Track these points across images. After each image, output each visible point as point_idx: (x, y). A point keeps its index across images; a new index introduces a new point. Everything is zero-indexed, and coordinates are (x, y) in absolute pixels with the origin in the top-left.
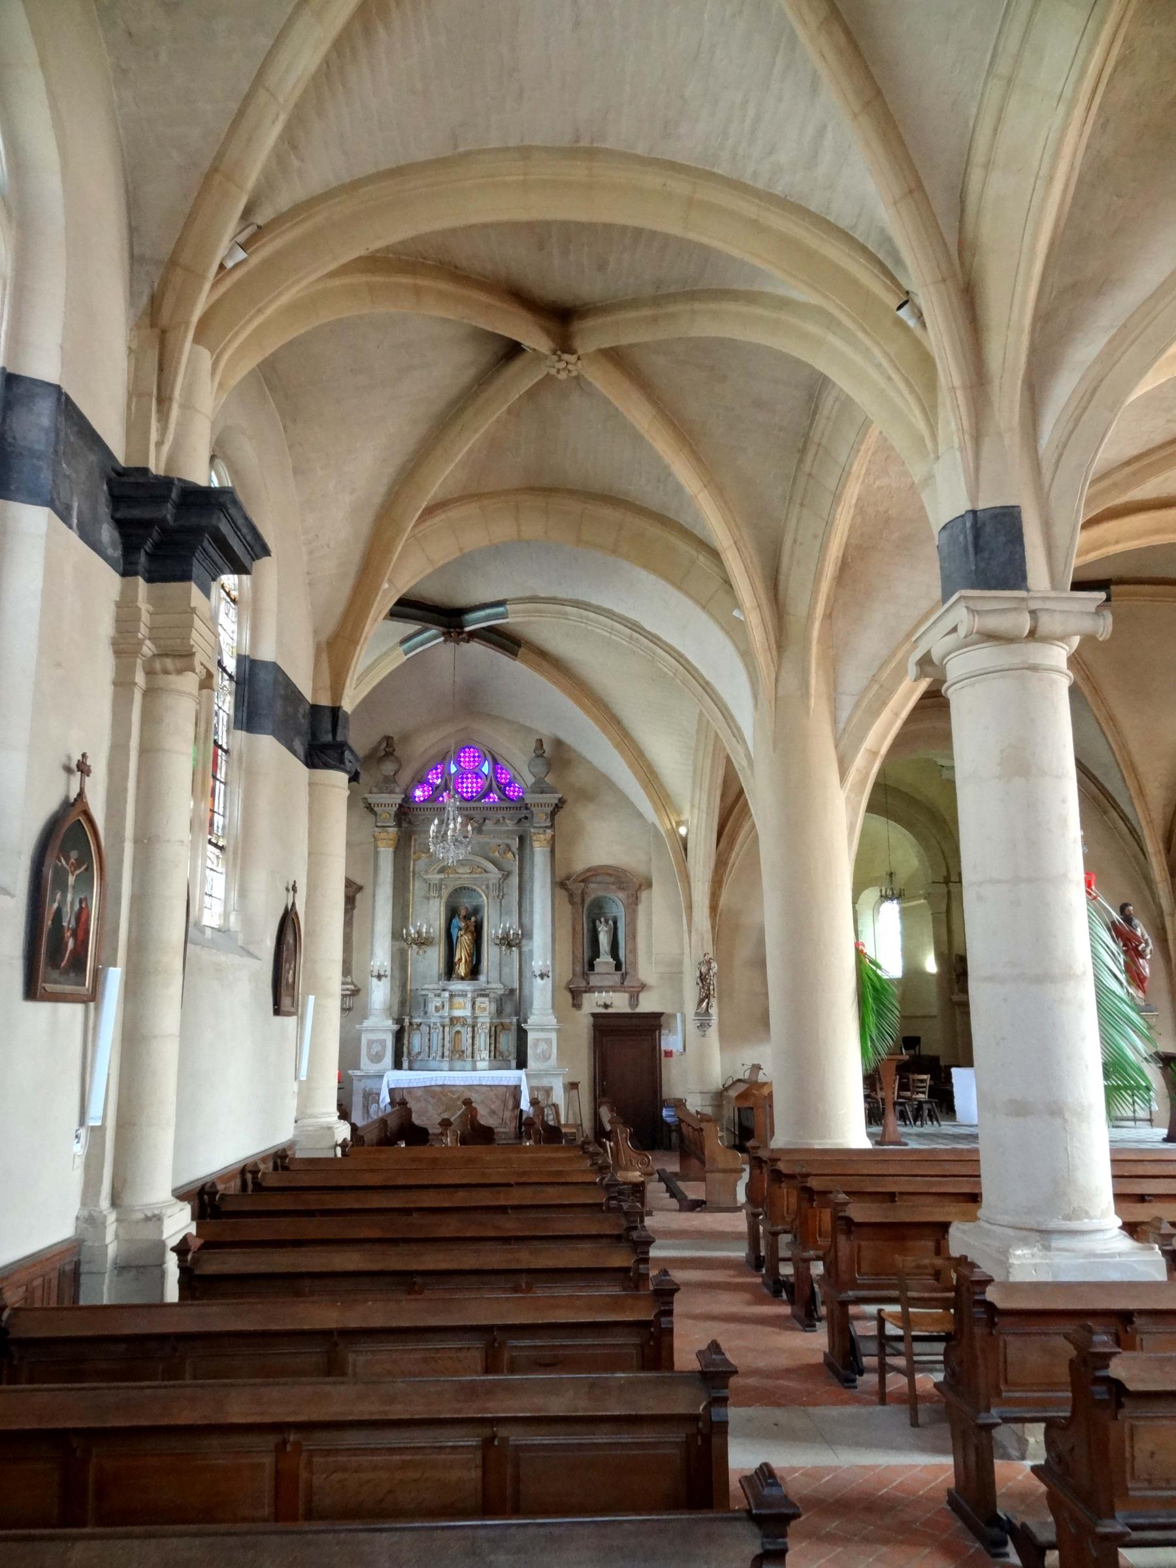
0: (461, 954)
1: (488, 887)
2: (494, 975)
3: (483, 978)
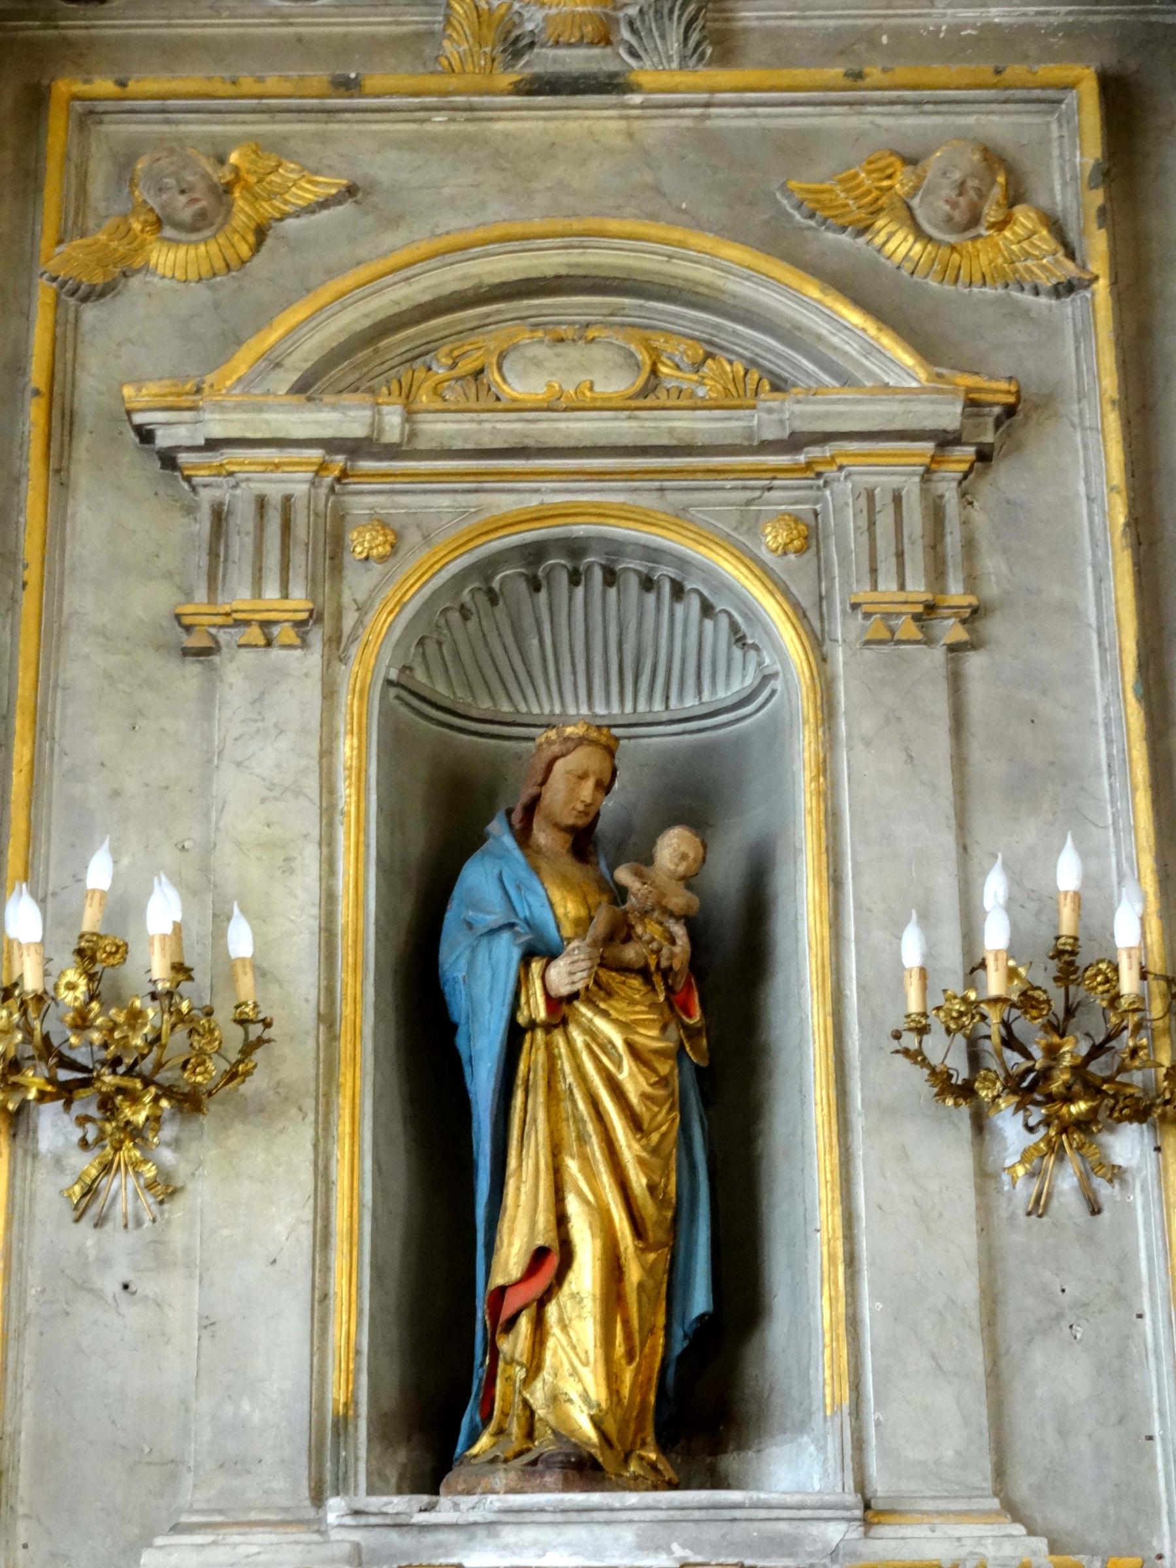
0: (573, 1195)
1: (810, 537)
2: (928, 1423)
3: (794, 1469)
